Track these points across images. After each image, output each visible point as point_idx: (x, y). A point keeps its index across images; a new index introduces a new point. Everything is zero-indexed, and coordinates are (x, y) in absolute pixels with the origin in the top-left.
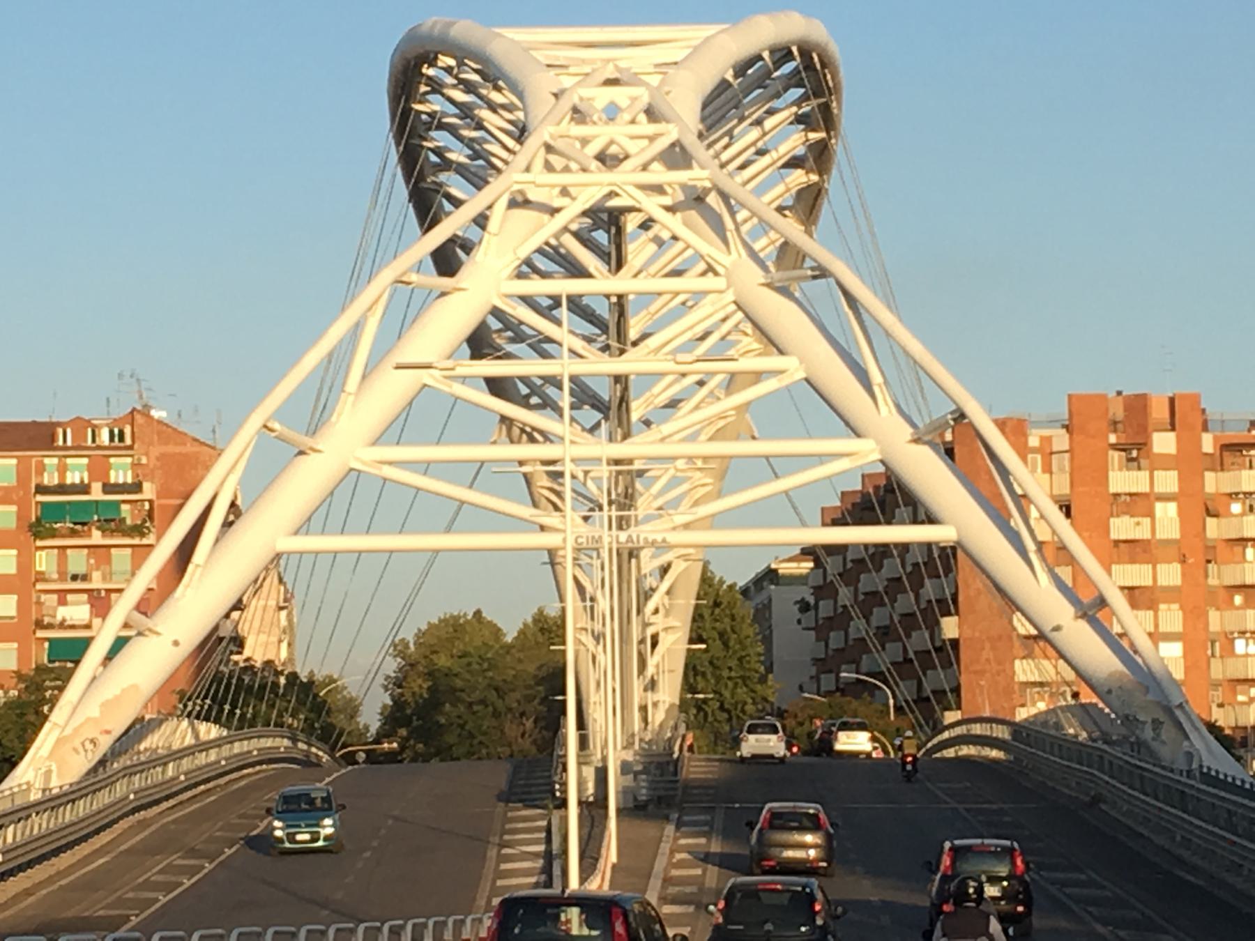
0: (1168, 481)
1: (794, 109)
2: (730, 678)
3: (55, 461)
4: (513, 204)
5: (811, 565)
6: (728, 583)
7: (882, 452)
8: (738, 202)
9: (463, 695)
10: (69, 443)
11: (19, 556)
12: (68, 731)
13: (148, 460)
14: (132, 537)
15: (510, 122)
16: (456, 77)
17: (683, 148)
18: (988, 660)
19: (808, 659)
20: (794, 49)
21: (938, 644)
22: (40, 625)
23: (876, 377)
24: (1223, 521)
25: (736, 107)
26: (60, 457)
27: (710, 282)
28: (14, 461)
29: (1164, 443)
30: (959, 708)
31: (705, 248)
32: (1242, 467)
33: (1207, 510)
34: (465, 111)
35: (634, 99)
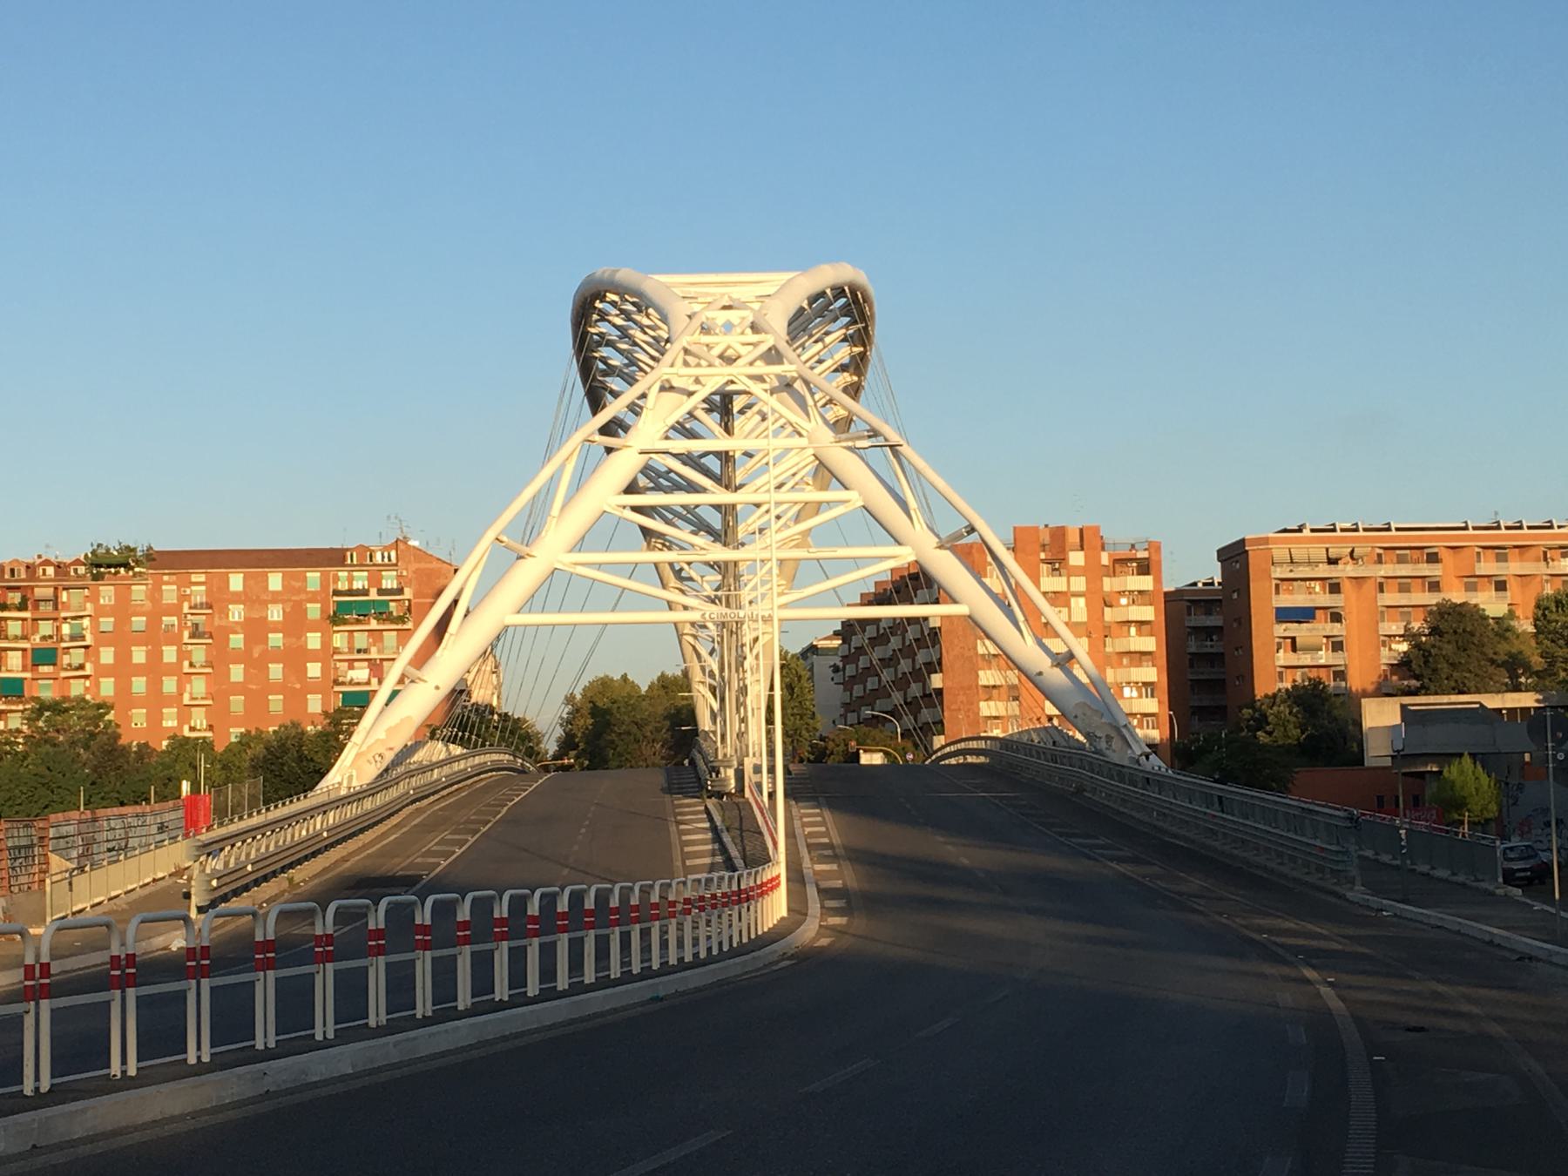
0: (1079, 584)
1: (844, 331)
2: (792, 715)
3: (346, 574)
4: (662, 389)
5: (840, 642)
7: (917, 555)
8: (815, 386)
9: (616, 728)
10: (355, 562)
11: (322, 637)
12: (364, 748)
14: (397, 624)
15: (653, 337)
16: (620, 310)
17: (777, 351)
18: (962, 702)
19: (839, 703)
20: (846, 288)
22: (336, 682)
23: (912, 503)
24: (1114, 609)
25: (804, 330)
26: (349, 571)
27: (796, 441)
28: (318, 574)
29: (1076, 558)
30: (943, 734)
31: (794, 418)
32: (1127, 574)
33: (1105, 602)
34: (624, 333)
35: (743, 318)
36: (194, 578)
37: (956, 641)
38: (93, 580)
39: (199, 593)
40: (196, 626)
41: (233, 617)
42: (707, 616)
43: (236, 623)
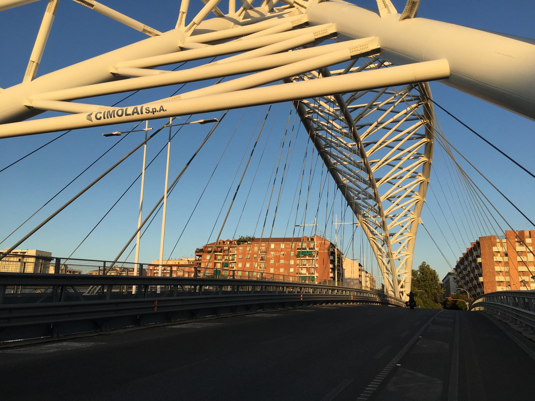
2: (434, 289)
6: (433, 270)
21: (479, 283)
22: (297, 273)
29: (528, 241)
36: (262, 245)
37: (487, 267)
38: (238, 245)
39: (263, 248)
40: (262, 257)
41: (272, 255)
42: (93, 117)
43: (272, 257)
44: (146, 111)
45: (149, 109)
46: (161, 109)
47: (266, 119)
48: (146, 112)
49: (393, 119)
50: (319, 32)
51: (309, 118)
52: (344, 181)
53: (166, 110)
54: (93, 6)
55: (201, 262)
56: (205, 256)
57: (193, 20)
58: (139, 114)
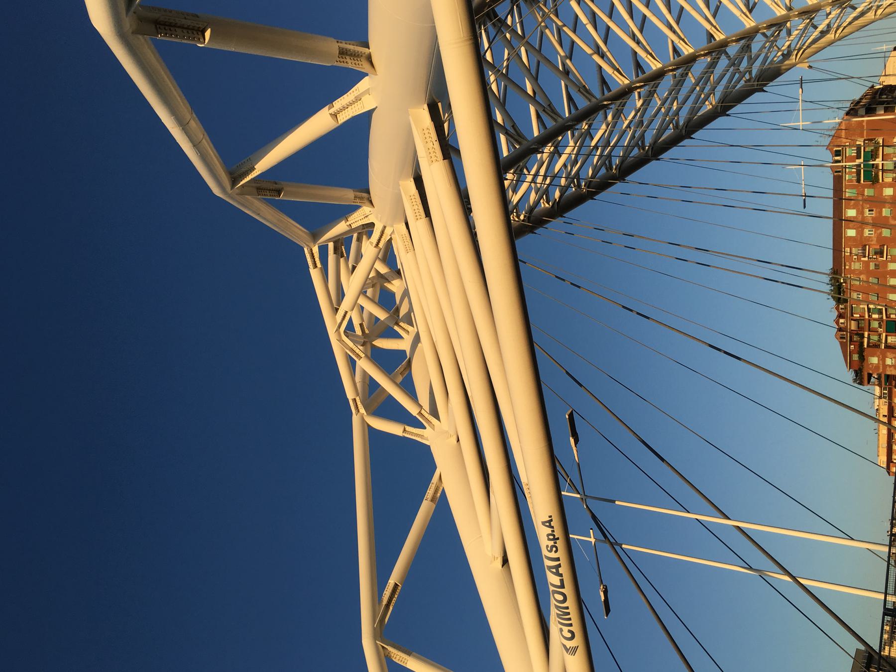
11: (886, 187)
13: (847, 142)
38: (847, 302)
41: (872, 234)
43: (875, 233)
44: (553, 551)
45: (550, 546)
46: (548, 524)
47: (579, 287)
48: (556, 552)
49: (587, 24)
50: (415, 210)
51: (589, 184)
52: (711, 104)
53: (550, 517)
54: (396, 585)
55: (883, 376)
56: (871, 366)
57: (414, 415)
58: (560, 564)
